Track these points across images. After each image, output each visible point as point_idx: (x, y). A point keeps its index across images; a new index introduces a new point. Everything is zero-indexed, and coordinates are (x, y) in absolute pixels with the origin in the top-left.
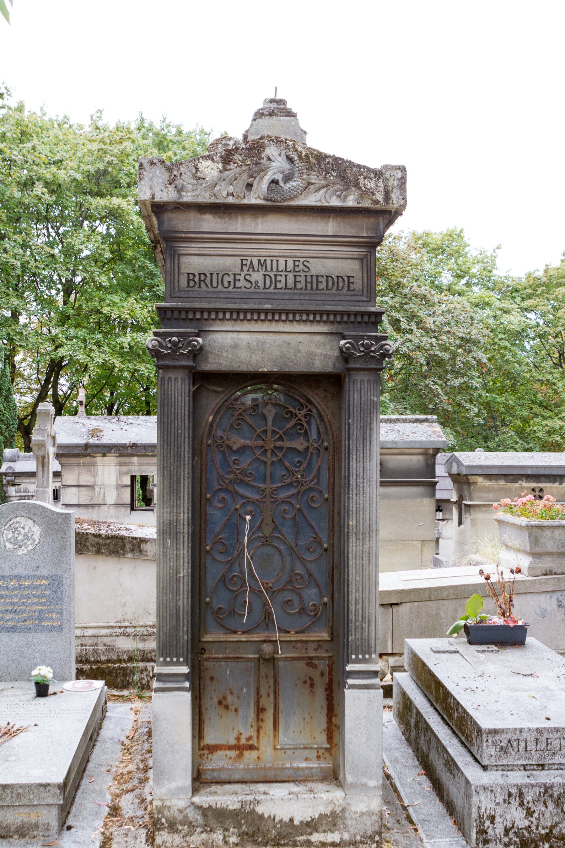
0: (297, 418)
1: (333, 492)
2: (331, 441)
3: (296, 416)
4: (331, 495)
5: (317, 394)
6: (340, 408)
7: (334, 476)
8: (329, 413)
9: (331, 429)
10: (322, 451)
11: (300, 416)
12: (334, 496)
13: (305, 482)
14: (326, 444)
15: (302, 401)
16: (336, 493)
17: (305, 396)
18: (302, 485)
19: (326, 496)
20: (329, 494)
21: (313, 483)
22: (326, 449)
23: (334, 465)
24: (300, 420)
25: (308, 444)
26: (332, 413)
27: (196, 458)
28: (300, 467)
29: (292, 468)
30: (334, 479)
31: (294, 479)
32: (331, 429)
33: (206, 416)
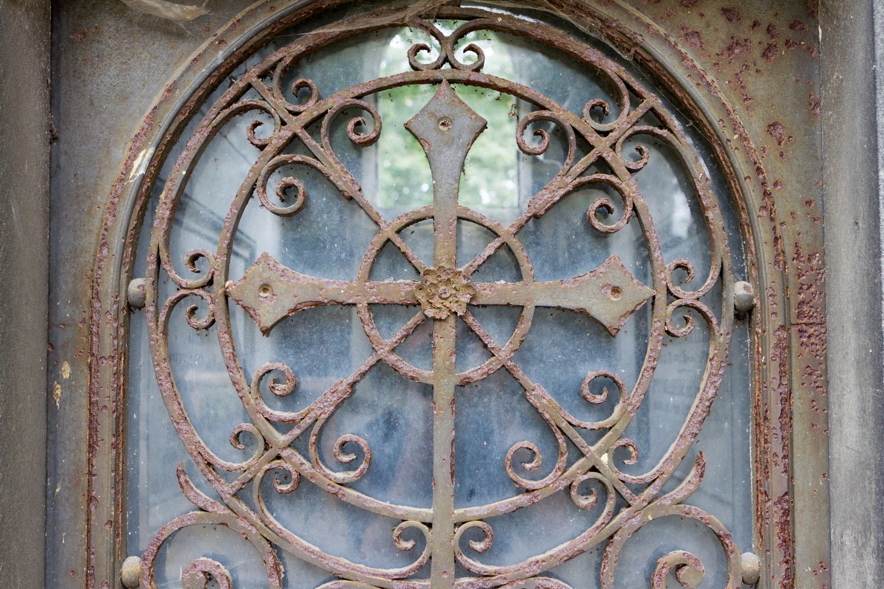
0: (591, 157)
1: (788, 543)
2: (770, 274)
3: (585, 146)
4: (778, 555)
5: (690, 35)
6: (811, 105)
7: (788, 456)
8: (754, 126)
9: (770, 210)
10: (724, 327)
11: (601, 146)
12: (790, 561)
13: (639, 489)
14: (739, 289)
15: (611, 67)
16: (800, 548)
17: (629, 42)
18: (622, 503)
19: (750, 561)
20: (765, 551)
21: (679, 492)
22: (744, 315)
23: (786, 399)
24: (602, 164)
25: (647, 291)
26: (772, 126)
27: (66, 371)
28: (607, 408)
29: (563, 415)
30: (789, 470)
31: (578, 472)
32: (770, 210)
33: (120, 153)
